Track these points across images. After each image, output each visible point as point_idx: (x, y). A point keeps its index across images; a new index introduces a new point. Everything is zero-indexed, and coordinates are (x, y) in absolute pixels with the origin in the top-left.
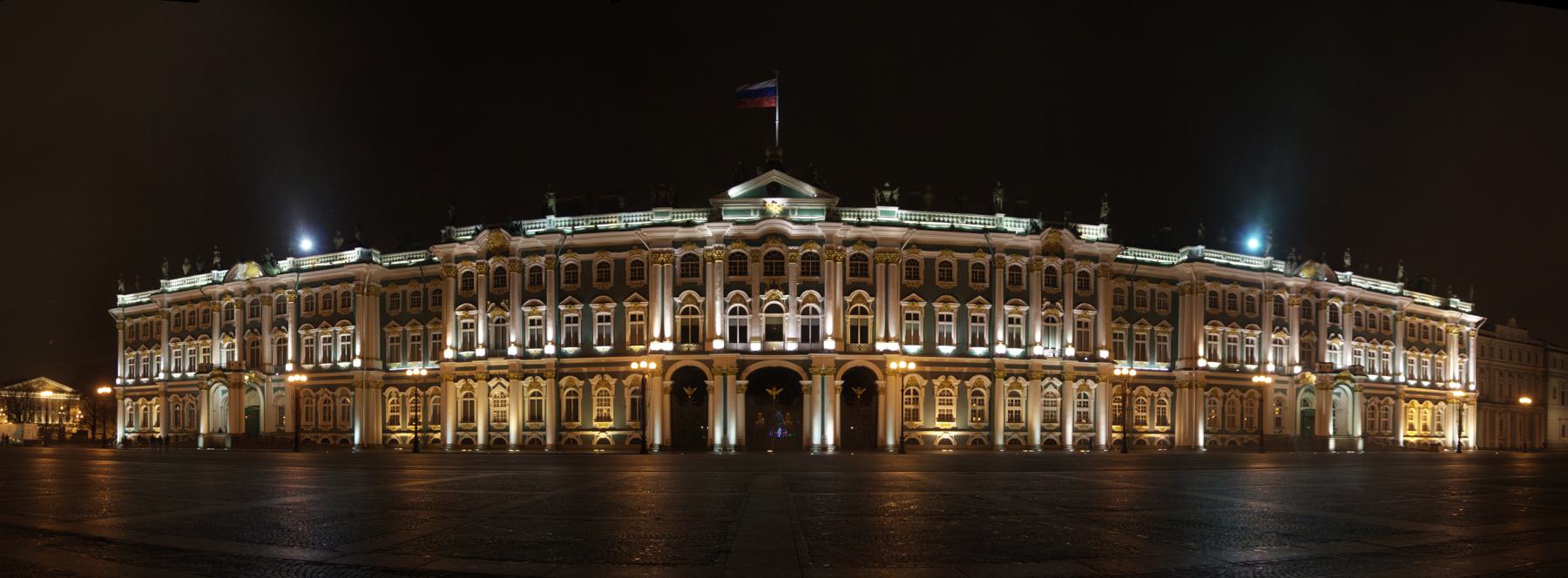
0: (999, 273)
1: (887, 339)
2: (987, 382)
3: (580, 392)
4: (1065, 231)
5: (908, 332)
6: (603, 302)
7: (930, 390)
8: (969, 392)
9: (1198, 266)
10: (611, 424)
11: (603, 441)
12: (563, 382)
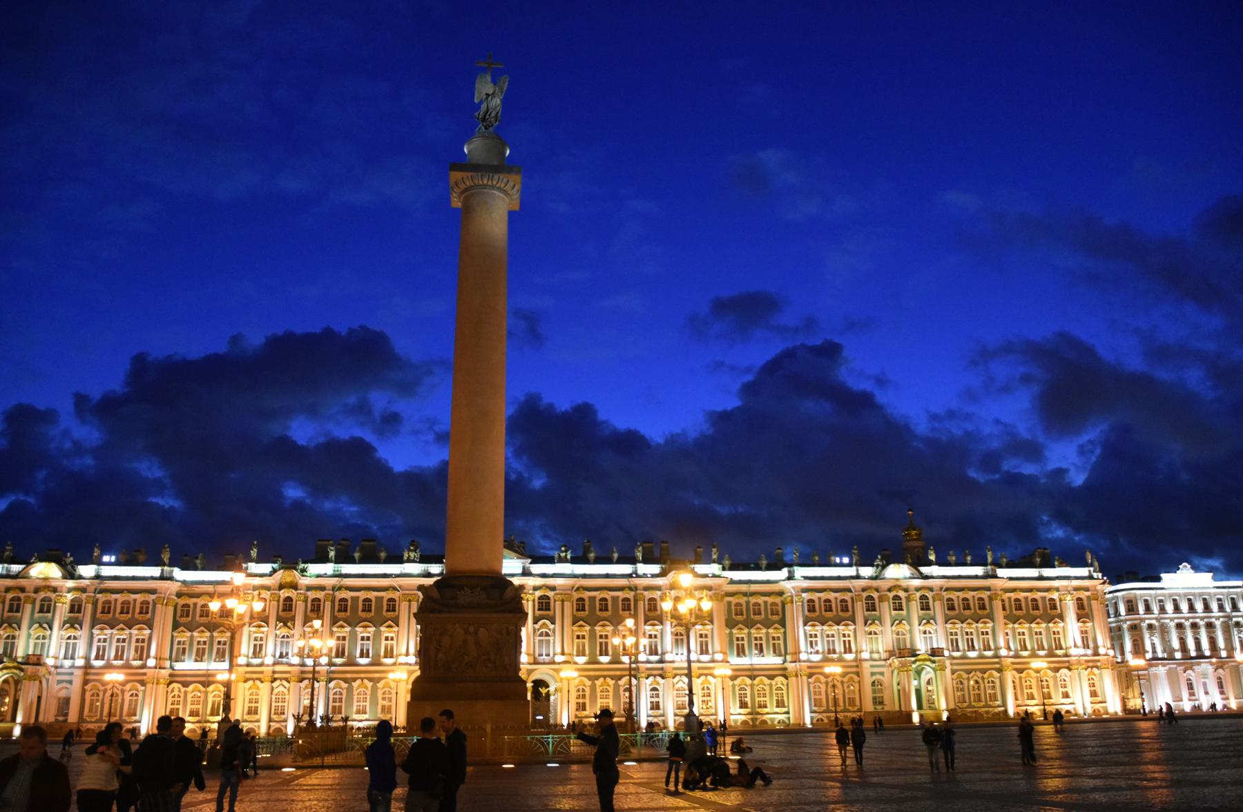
1: (563, 653)
3: (344, 692)
7: (593, 687)
8: (622, 689)
10: (366, 716)
12: (332, 685)
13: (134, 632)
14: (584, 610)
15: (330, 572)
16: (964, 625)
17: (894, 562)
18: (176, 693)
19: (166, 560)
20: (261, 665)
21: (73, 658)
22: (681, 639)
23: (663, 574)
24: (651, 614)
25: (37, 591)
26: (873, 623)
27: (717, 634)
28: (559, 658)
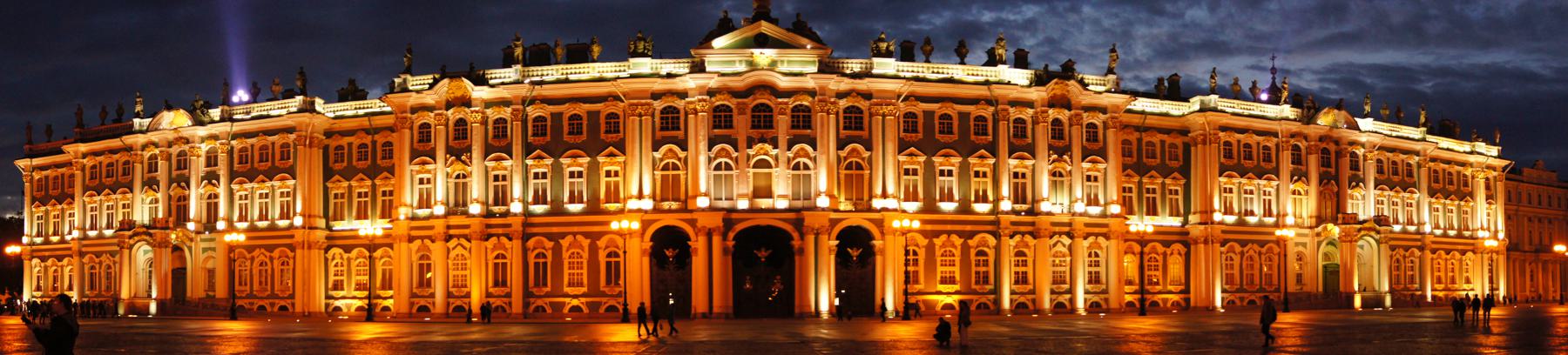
0: (1002, 125)
1: (884, 195)
2: (992, 241)
3: (549, 254)
4: (1072, 82)
5: (907, 188)
6: (575, 156)
7: (930, 249)
8: (973, 252)
9: (1211, 116)
11: (575, 309)
12: (531, 243)
18: (338, 260)
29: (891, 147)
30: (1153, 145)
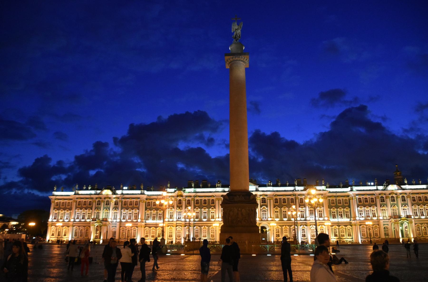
1: (271, 217)
3: (199, 230)
6: (205, 209)
7: (282, 229)
8: (292, 230)
12: (195, 228)
13: (134, 211)
14: (277, 202)
15: (193, 191)
16: (419, 207)
17: (391, 184)
18: (147, 230)
19: (142, 188)
20: (173, 221)
21: (116, 219)
22: (311, 213)
23: (305, 190)
24: (301, 204)
25: (105, 198)
26: (384, 206)
27: (325, 211)
28: (269, 219)
29: (272, 206)
30: (340, 200)
